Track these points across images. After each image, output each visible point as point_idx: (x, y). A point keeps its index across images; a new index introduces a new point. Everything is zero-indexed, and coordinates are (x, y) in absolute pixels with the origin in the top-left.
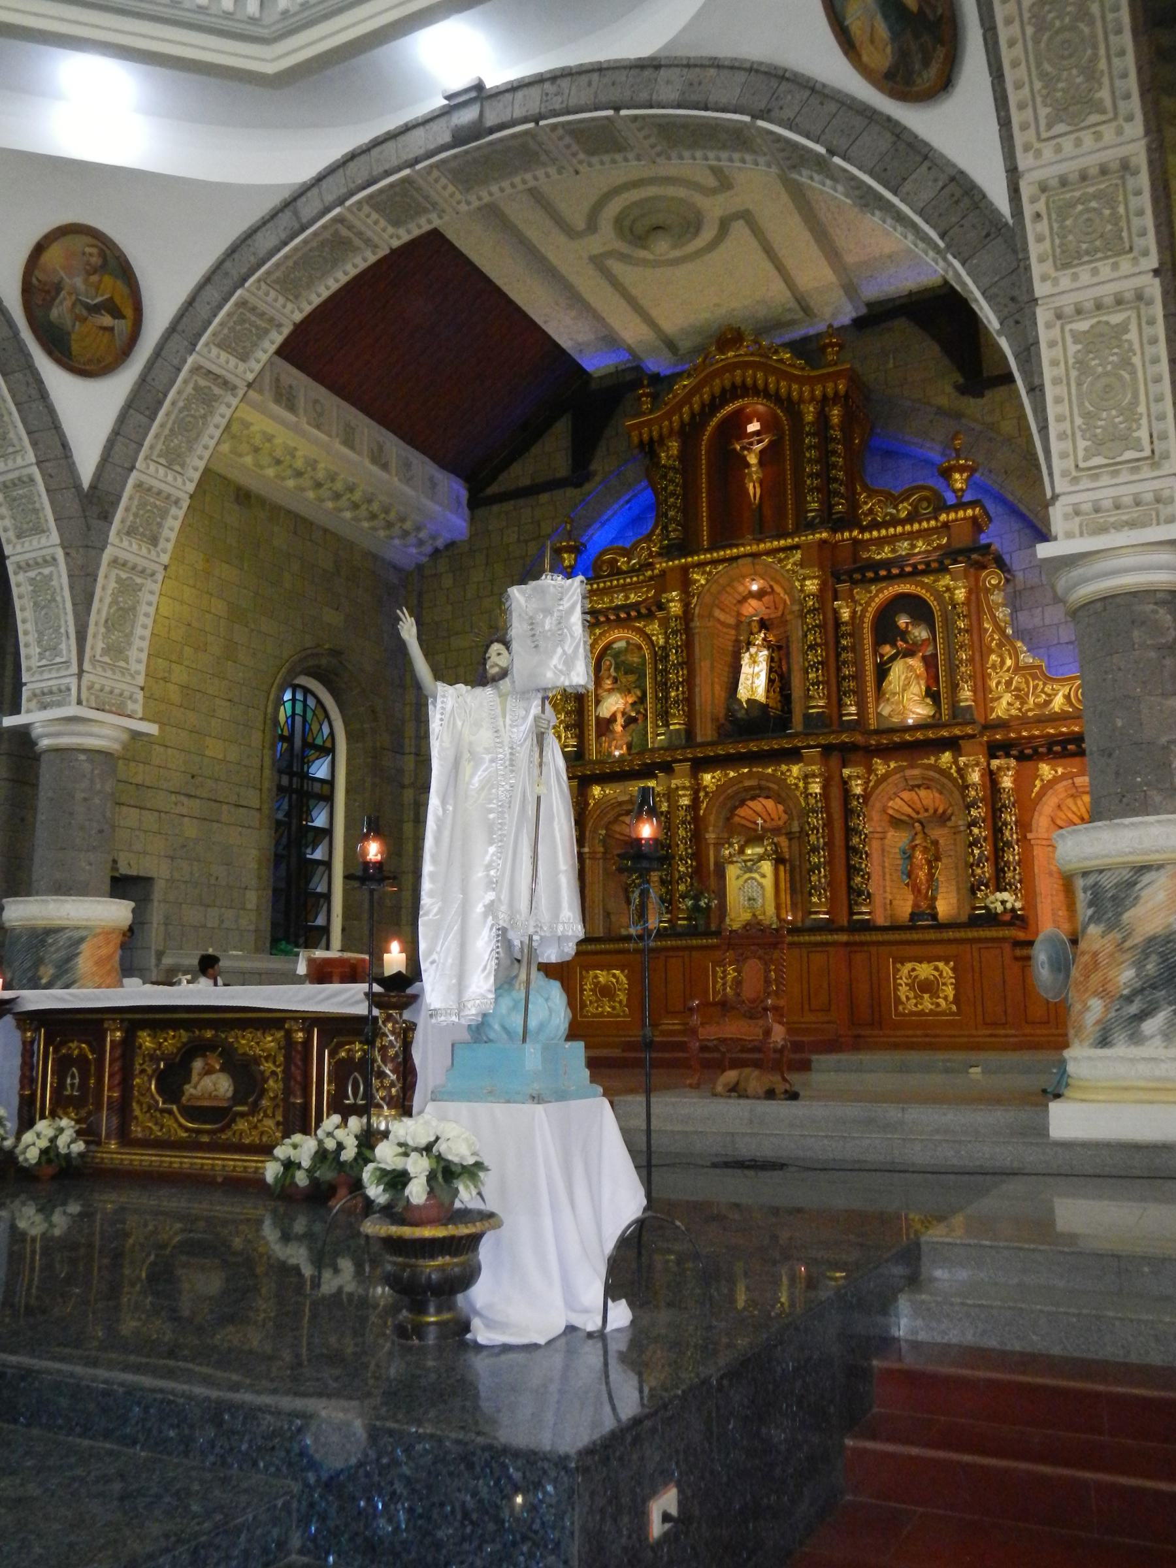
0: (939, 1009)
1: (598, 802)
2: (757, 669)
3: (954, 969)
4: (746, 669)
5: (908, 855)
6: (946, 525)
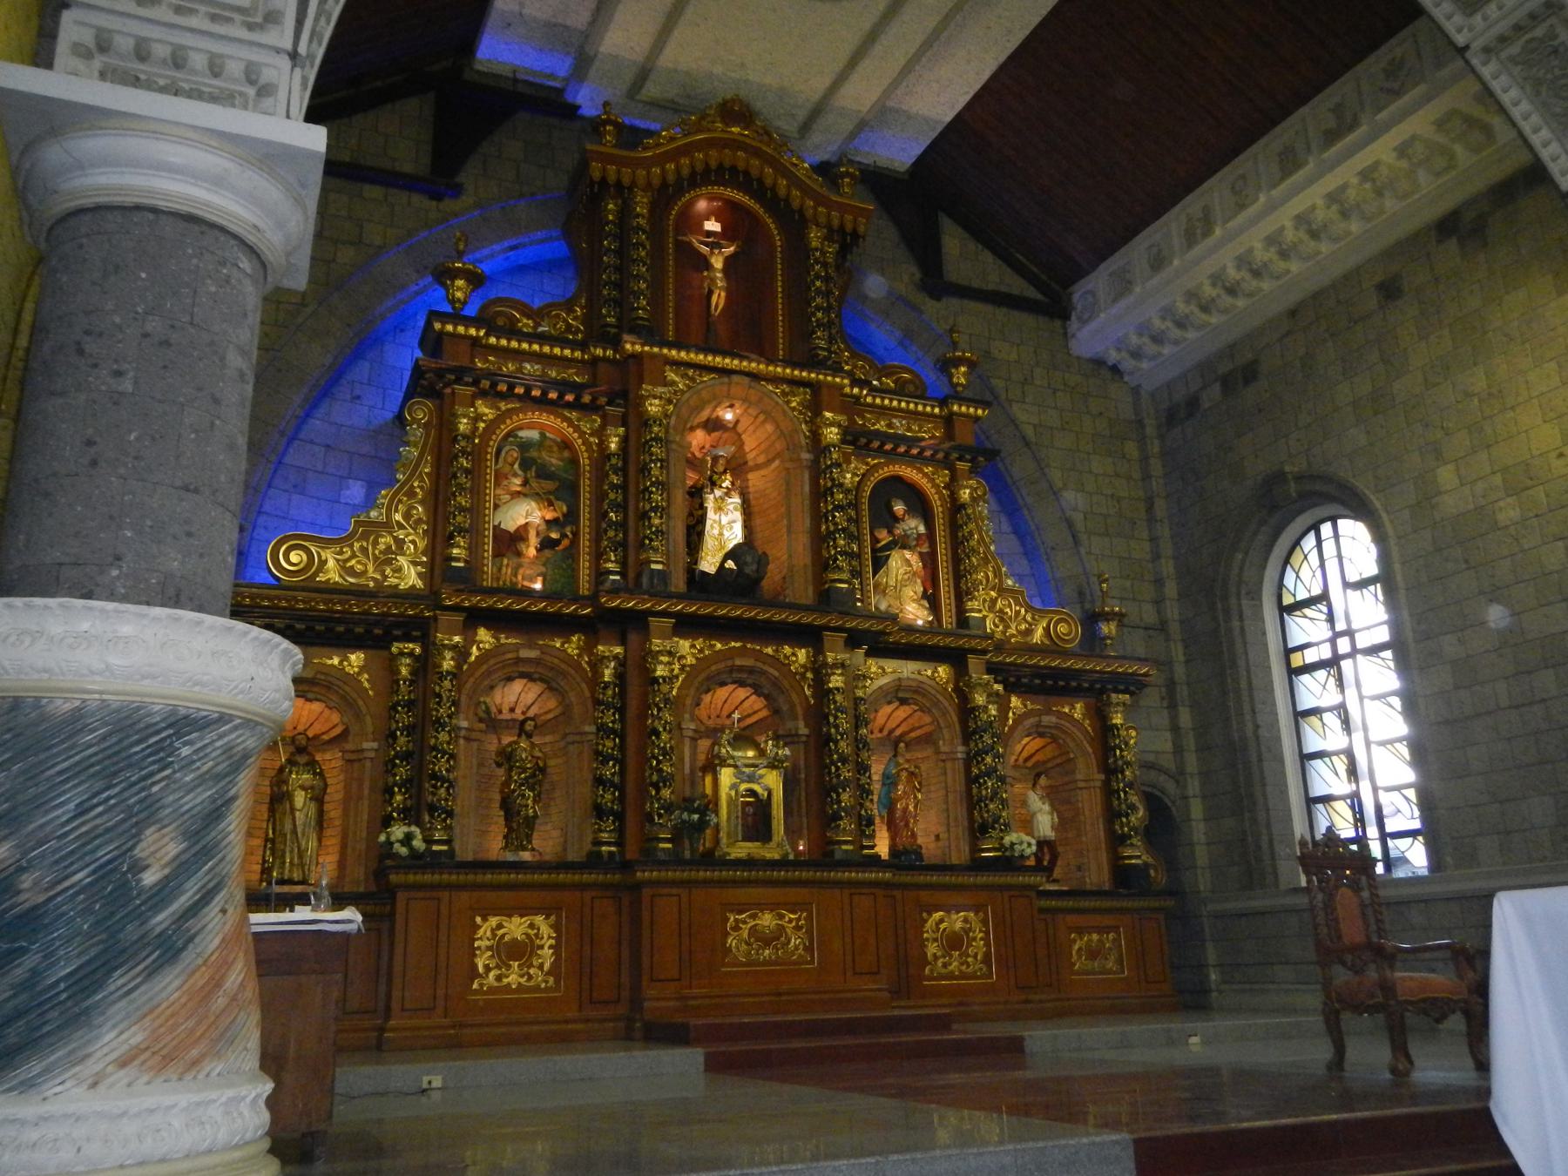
1: (485, 656)
2: (725, 520)
4: (711, 515)
5: (889, 781)
6: (952, 414)
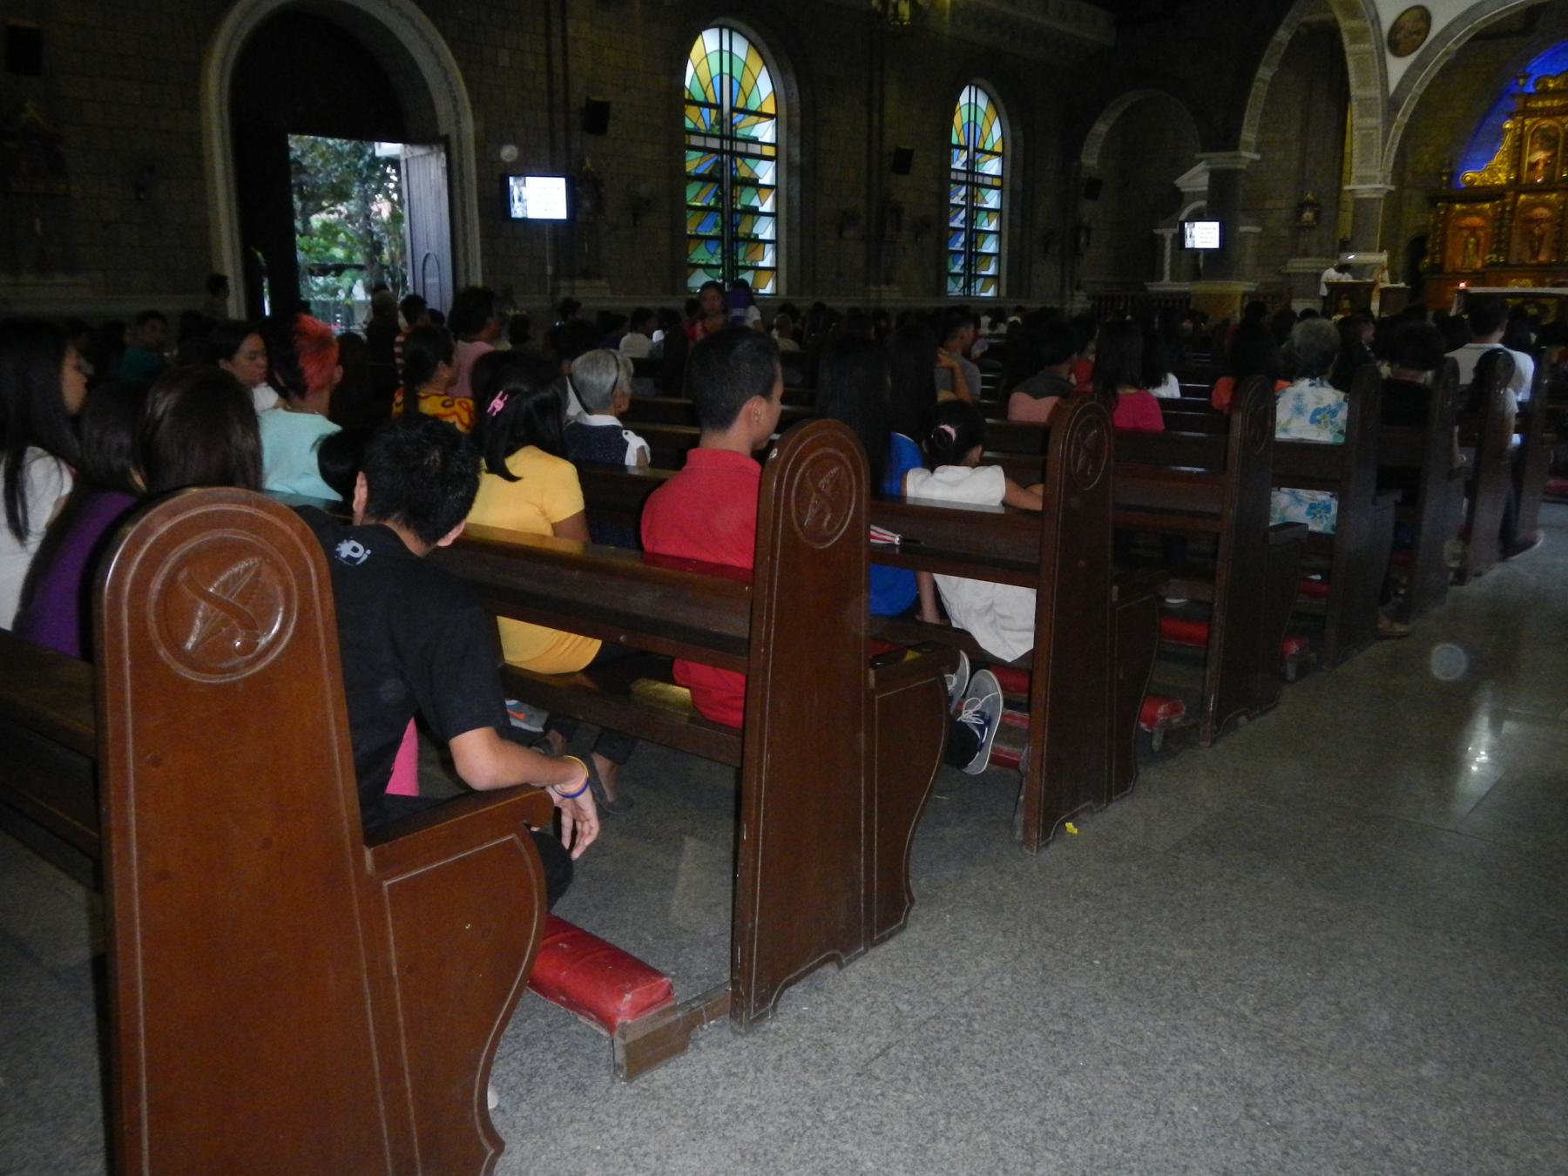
1: (1523, 202)
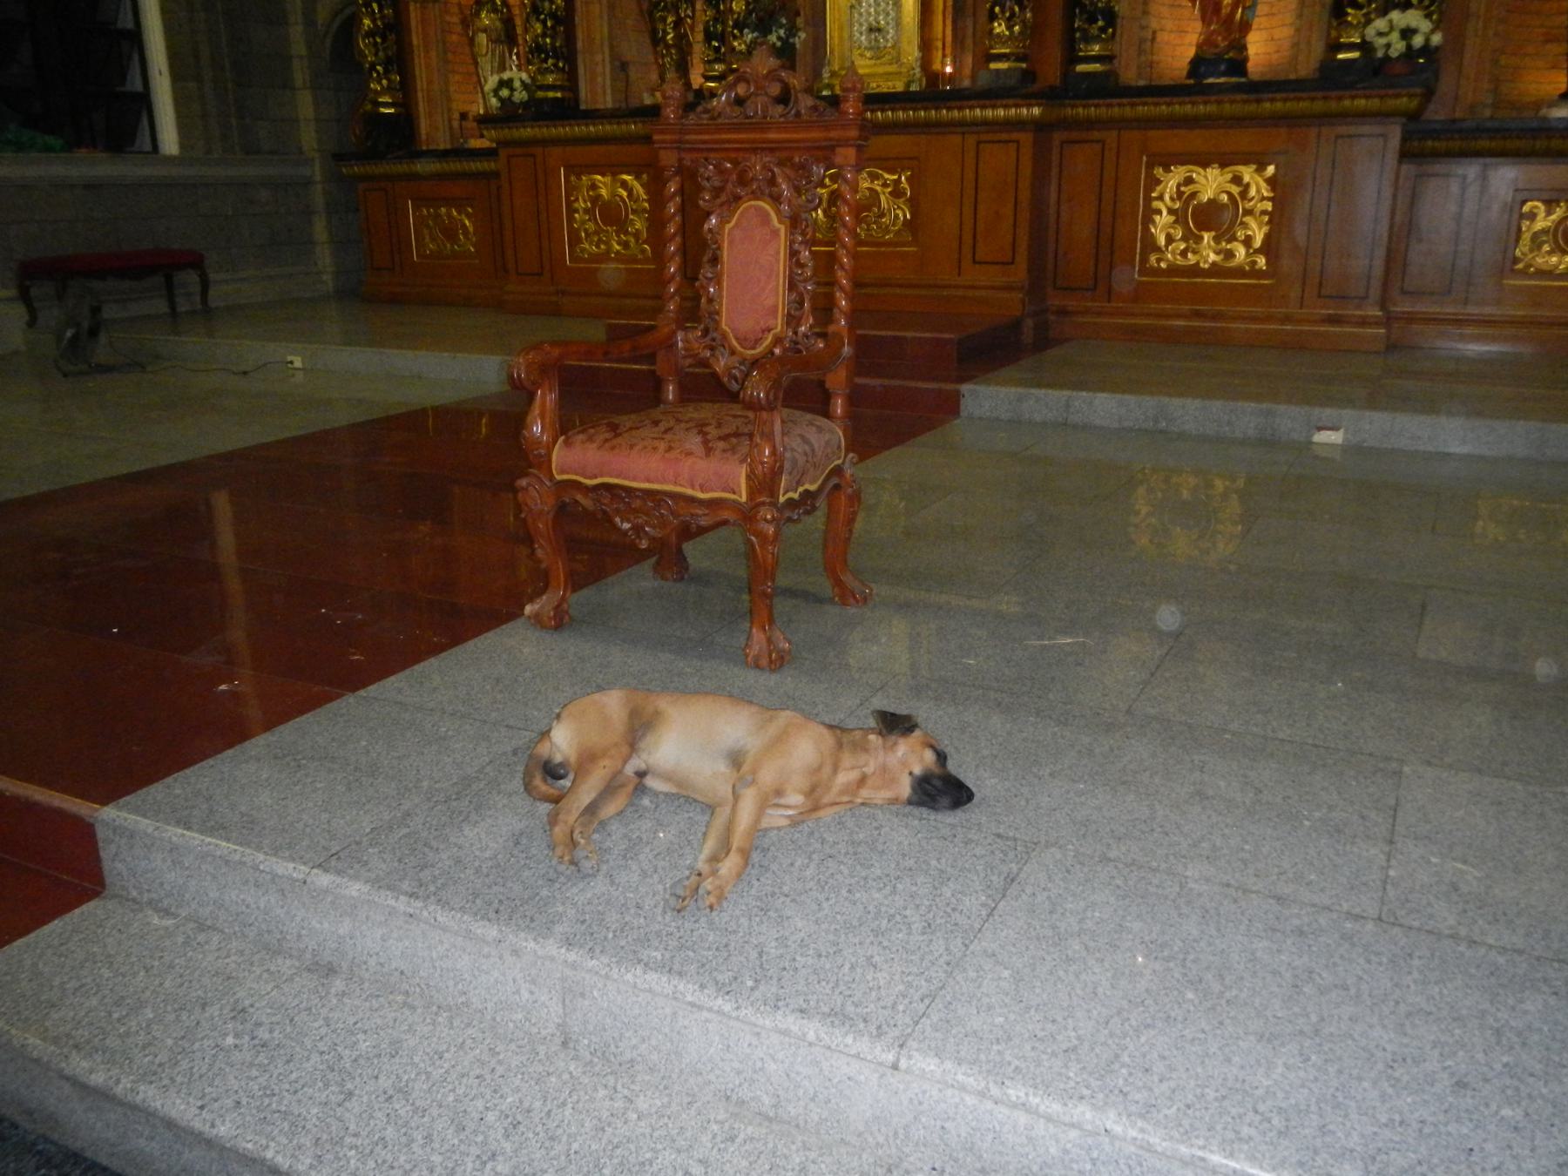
0: (1233, 263)
3: (1271, 182)
